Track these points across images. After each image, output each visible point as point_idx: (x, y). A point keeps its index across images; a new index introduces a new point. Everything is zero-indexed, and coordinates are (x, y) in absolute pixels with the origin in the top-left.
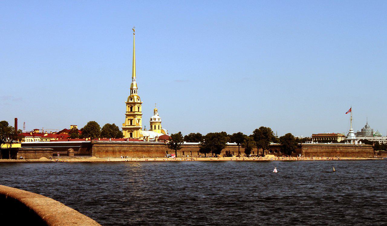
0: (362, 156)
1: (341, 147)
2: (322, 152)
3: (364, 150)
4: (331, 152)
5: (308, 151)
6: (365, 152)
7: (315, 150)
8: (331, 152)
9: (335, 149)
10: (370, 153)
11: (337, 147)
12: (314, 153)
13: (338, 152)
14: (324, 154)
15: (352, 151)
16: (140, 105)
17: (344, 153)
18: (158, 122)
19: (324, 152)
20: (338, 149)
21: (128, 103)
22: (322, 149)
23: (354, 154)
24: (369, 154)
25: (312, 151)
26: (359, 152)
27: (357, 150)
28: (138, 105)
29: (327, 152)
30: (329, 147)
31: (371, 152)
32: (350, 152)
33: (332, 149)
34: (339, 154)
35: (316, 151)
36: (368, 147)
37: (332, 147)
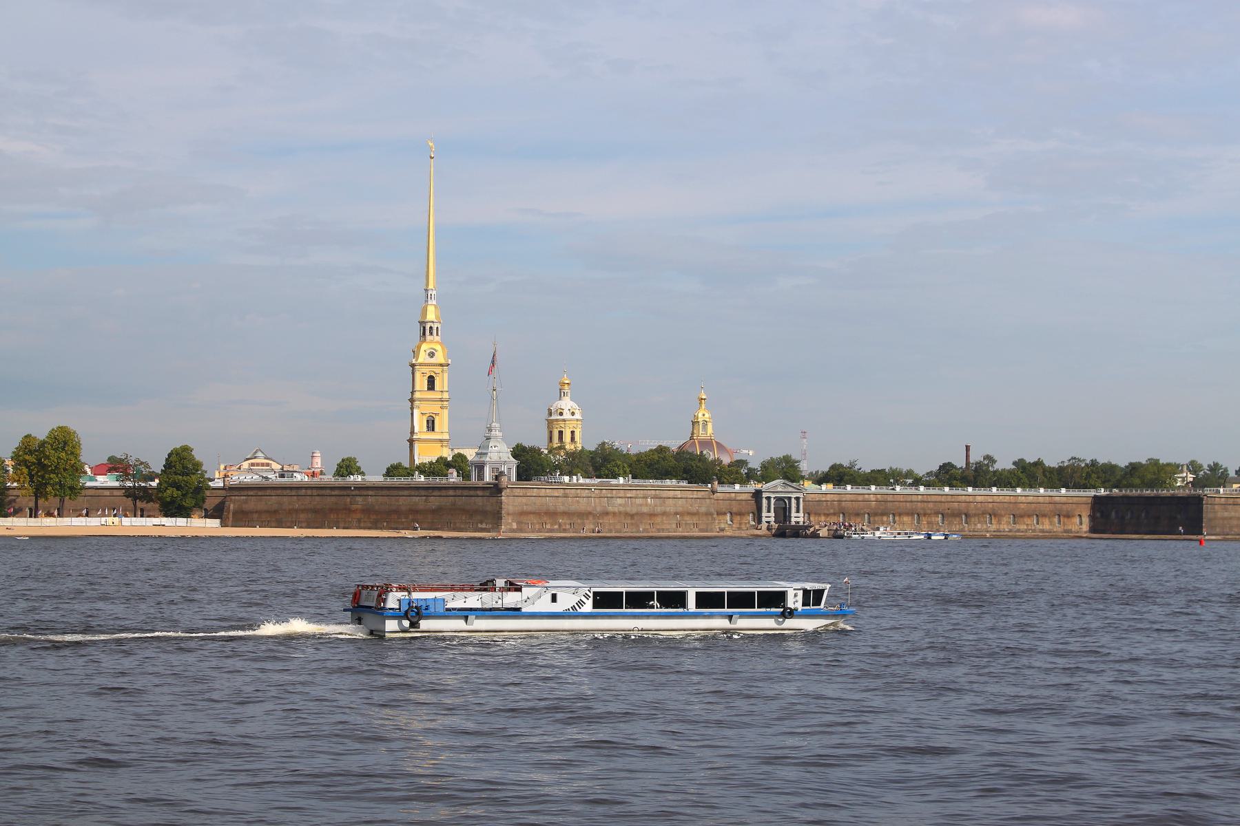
1: (370, 493)
2: (297, 511)
3: (461, 501)
4: (331, 510)
5: (246, 507)
6: (464, 511)
7: (272, 501)
9: (348, 500)
11: (357, 492)
12: (267, 512)
13: (355, 511)
14: (302, 516)
16: (438, 370)
19: (303, 511)
20: (359, 499)
24: (479, 517)
25: (261, 506)
26: (437, 511)
27: (434, 502)
28: (425, 369)
29: (315, 511)
30: (323, 492)
31: (489, 508)
32: (403, 508)
34: (358, 516)
36: (479, 493)
37: (336, 492)
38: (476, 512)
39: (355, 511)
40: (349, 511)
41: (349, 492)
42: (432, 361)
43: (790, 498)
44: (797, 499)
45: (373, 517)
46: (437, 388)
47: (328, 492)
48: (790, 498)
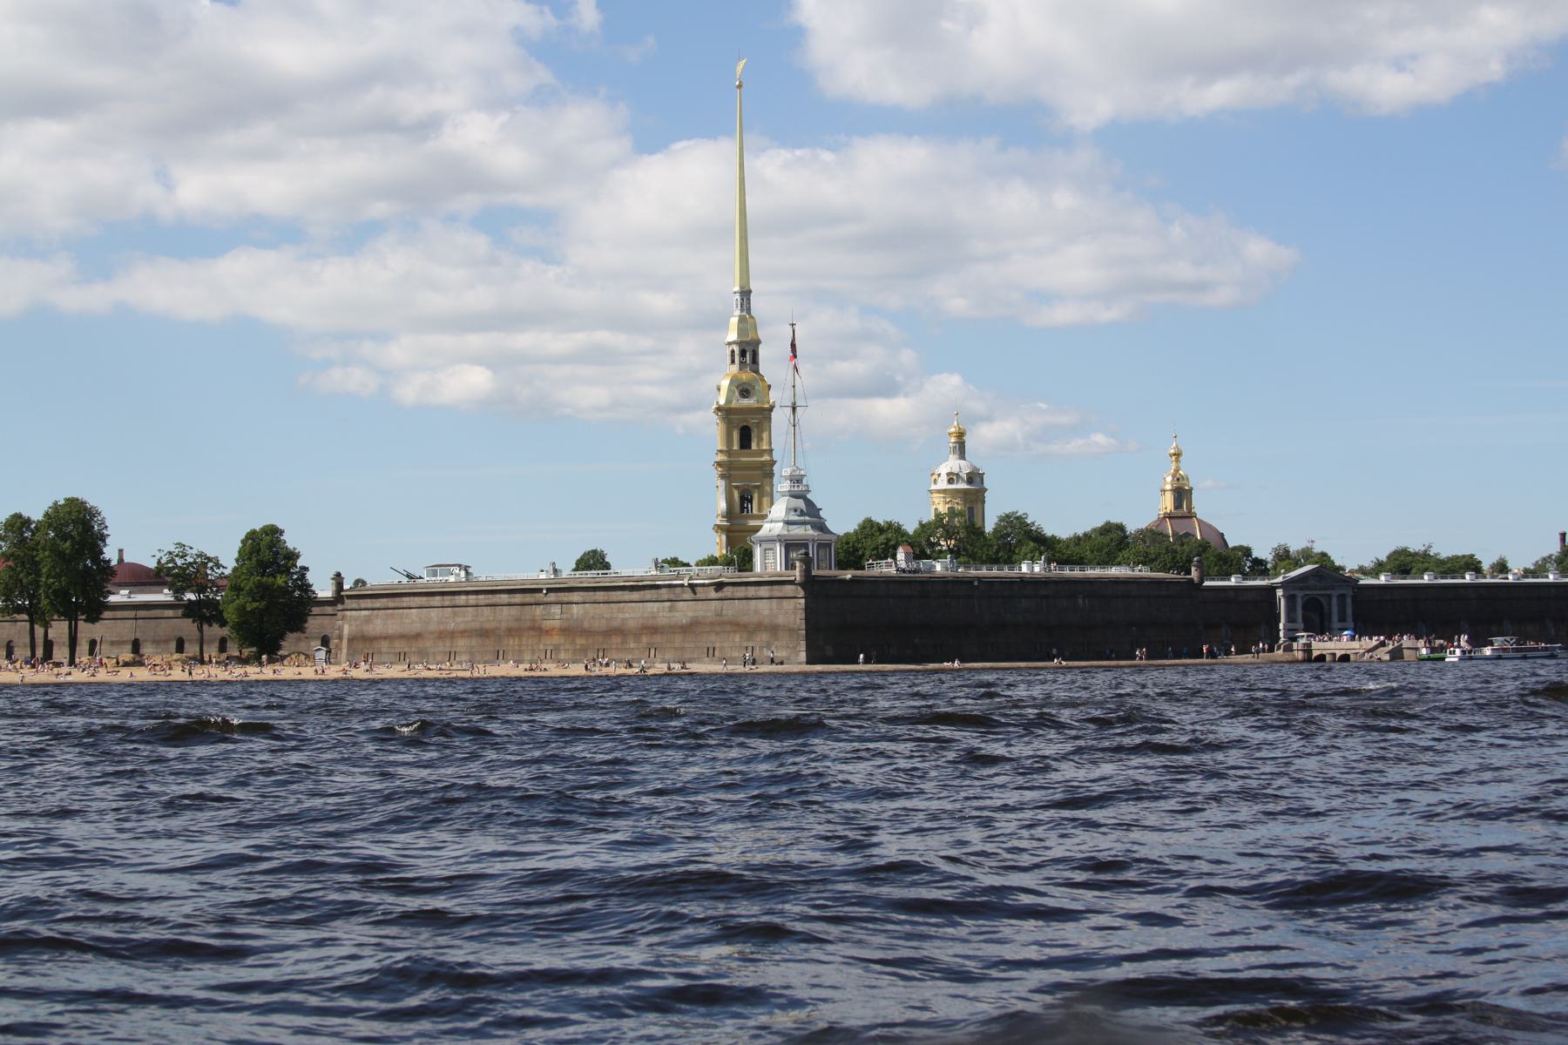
0: (710, 652)
1: (575, 597)
2: (452, 635)
3: (731, 609)
4: (511, 632)
6: (737, 626)
8: (511, 632)
9: (539, 610)
10: (774, 629)
11: (552, 597)
12: (402, 637)
13: (548, 632)
14: (462, 643)
15: (651, 622)
17: (586, 633)
18: (944, 491)
19: (463, 633)
20: (556, 609)
21: (726, 412)
22: (455, 614)
23: (658, 639)
25: (393, 627)
29: (484, 633)
31: (781, 620)
32: (632, 624)
33: (514, 611)
34: (556, 639)
35: (417, 627)
37: (518, 598)
38: (759, 627)
39: (548, 632)
40: (539, 631)
41: (539, 597)
42: (746, 402)
43: (1330, 596)
44: (1342, 597)
45: (580, 641)
46: (754, 447)
47: (504, 598)
48: (1330, 596)
